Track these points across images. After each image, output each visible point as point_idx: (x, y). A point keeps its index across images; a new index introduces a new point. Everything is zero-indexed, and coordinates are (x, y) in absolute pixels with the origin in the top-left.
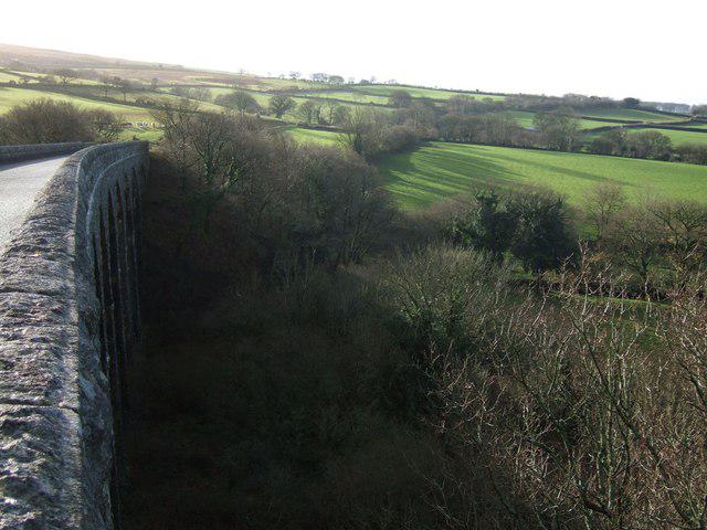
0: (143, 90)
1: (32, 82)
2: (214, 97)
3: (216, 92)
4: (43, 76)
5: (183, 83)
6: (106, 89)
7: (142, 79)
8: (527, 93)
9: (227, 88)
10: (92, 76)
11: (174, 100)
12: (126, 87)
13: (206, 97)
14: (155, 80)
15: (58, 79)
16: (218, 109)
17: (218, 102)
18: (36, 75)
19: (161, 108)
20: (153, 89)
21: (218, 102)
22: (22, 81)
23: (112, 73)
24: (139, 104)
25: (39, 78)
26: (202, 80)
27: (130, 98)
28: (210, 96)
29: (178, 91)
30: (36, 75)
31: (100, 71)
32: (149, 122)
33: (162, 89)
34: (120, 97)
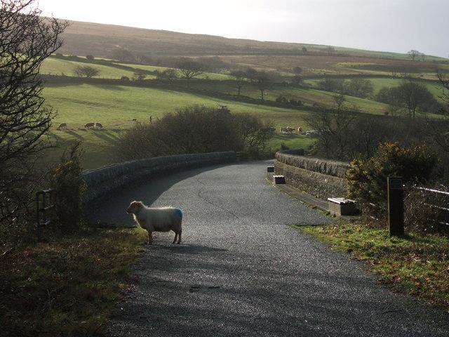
0: (284, 85)
1: (148, 77)
2: (377, 91)
3: (379, 84)
4: (162, 69)
5: (334, 73)
6: (239, 84)
7: (279, 68)
8: (383, 51)
9: (394, 77)
10: (219, 66)
11: (326, 99)
12: (263, 82)
13: (363, 92)
14: (298, 70)
15: (180, 73)
16: (378, 108)
17: (381, 98)
18: (151, 68)
19: (307, 109)
20: (297, 83)
21: (381, 98)
22: (137, 77)
23: (244, 62)
24: (280, 103)
25: (156, 73)
26: (360, 67)
27: (270, 96)
28: (371, 90)
29: (328, 84)
30: (151, 68)
31: (226, 59)
32: (298, 126)
33: (307, 81)
34: (256, 95)
